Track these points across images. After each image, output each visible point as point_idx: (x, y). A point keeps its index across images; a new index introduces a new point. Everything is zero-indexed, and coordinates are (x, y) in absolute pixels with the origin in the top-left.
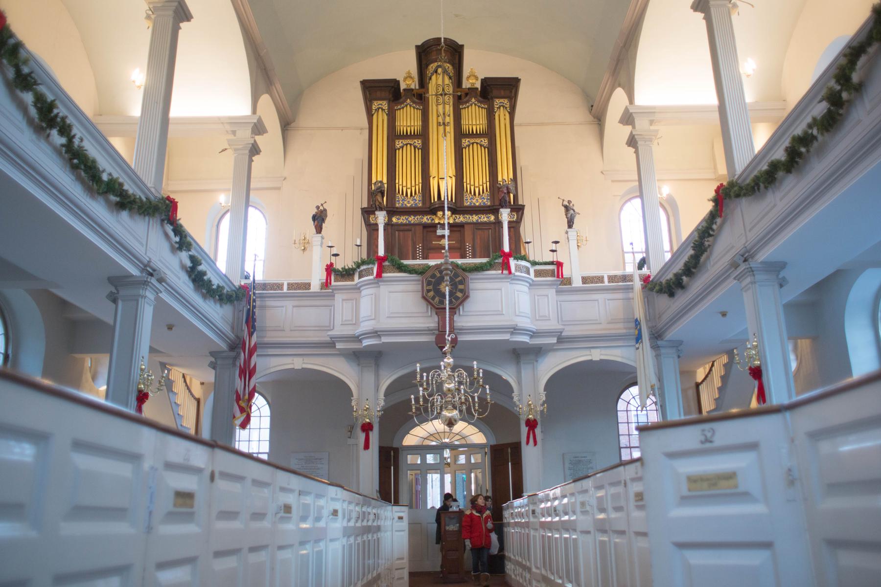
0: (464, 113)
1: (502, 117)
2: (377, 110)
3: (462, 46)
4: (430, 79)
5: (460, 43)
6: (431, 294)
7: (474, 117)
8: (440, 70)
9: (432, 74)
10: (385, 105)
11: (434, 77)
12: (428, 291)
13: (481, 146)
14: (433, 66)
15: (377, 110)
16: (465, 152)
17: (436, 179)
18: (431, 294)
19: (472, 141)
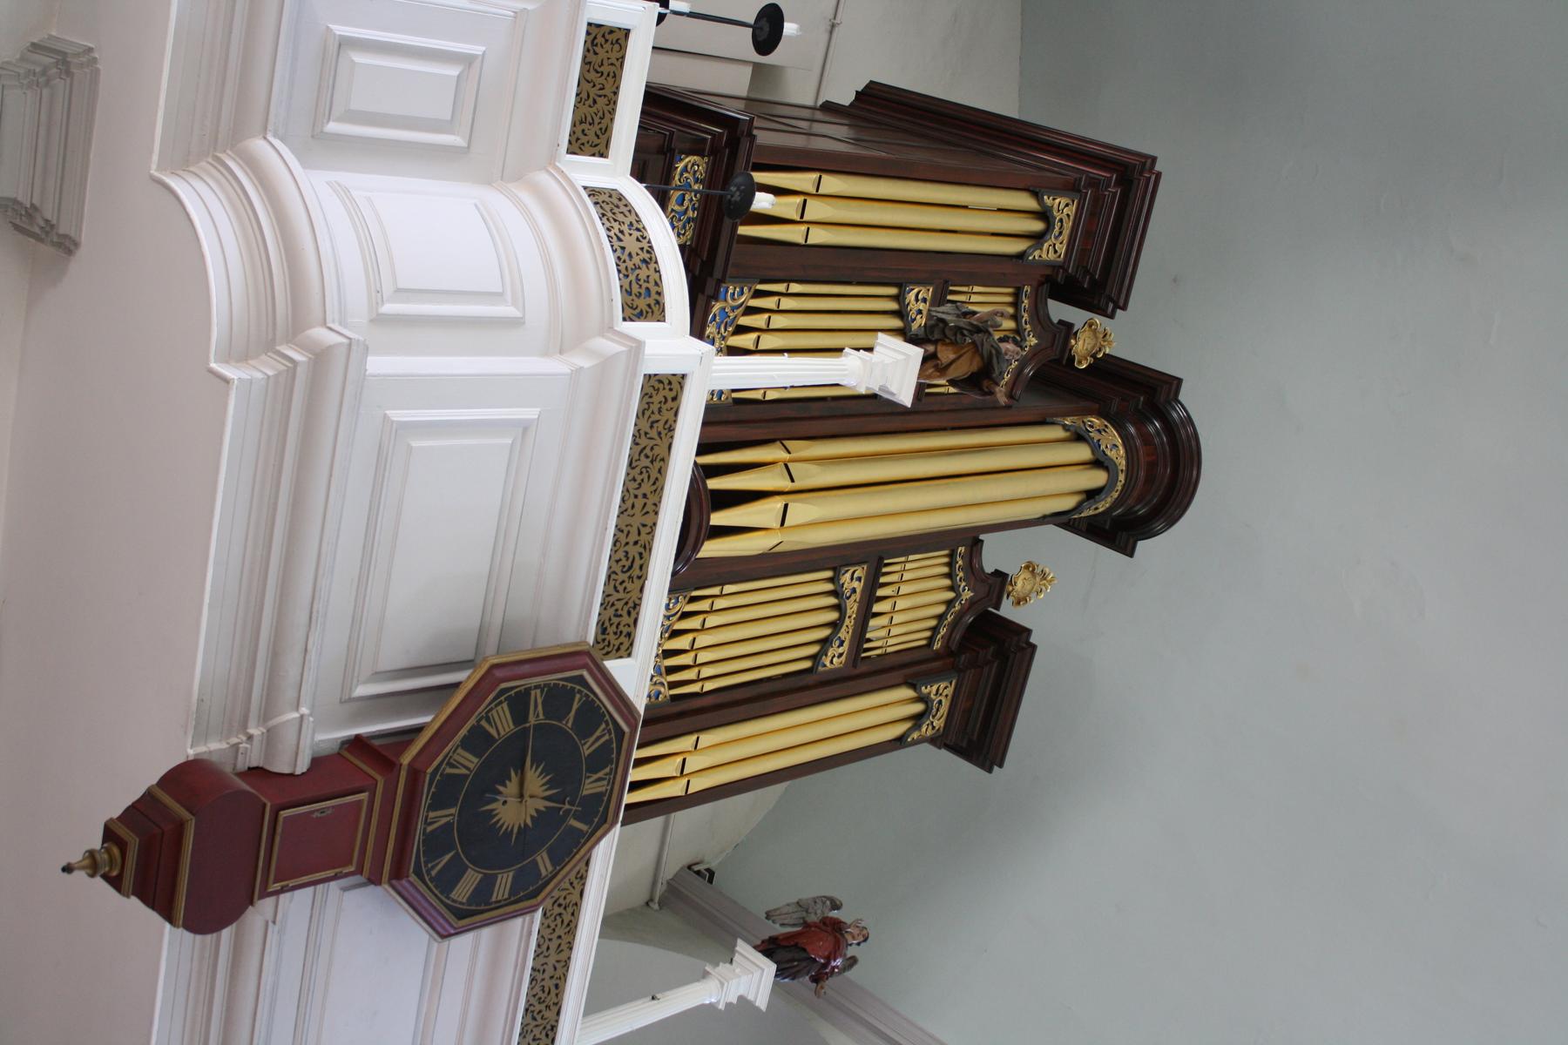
0: (936, 563)
1: (882, 711)
2: (1044, 215)
3: (1129, 551)
4: (1079, 437)
5: (1142, 546)
6: (502, 724)
7: (913, 606)
8: (1098, 478)
9: (1095, 447)
10: (1053, 251)
11: (1083, 452)
12: (519, 704)
13: (825, 643)
14: (1113, 444)
15: (1044, 215)
16: (816, 582)
17: (783, 483)
18: (502, 724)
19: (852, 607)
